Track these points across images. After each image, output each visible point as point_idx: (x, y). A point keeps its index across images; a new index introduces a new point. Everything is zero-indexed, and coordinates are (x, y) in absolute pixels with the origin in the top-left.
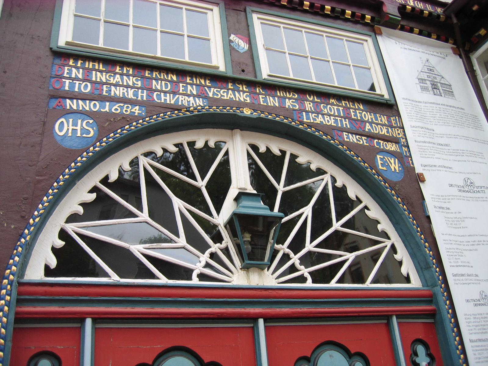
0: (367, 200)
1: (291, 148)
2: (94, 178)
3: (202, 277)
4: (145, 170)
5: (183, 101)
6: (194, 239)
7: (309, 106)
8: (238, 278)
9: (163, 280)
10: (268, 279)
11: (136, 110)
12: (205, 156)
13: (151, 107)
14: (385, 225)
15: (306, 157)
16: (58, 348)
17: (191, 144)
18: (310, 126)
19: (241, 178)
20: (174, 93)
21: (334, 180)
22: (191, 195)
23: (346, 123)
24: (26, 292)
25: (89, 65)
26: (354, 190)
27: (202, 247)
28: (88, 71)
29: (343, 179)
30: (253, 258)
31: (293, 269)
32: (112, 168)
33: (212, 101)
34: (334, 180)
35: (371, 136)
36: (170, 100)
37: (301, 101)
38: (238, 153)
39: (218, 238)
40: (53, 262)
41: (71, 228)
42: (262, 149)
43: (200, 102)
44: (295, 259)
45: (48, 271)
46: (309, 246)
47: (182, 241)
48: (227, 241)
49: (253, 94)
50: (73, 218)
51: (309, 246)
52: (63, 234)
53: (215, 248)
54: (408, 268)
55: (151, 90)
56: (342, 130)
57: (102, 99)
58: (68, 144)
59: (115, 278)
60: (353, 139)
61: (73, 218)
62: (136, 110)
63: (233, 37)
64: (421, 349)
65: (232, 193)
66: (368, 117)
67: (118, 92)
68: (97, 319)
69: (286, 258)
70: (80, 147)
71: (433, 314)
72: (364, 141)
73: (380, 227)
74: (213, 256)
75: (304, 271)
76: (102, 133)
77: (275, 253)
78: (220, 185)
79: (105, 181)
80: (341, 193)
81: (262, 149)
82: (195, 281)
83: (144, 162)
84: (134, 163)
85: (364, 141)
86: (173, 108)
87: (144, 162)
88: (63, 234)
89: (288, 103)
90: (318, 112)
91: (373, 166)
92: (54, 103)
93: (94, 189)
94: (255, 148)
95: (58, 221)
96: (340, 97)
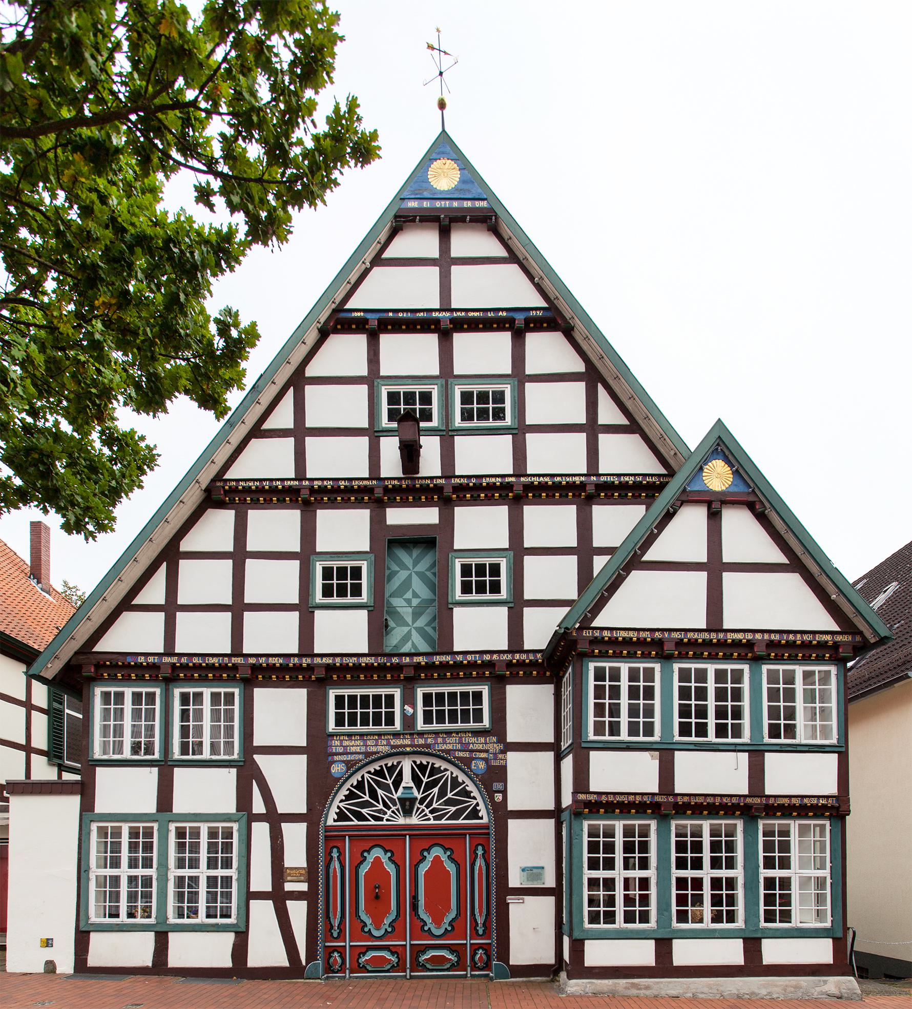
0: (468, 782)
1: (432, 760)
2: (348, 785)
3: (387, 820)
4: (368, 781)
5: (380, 748)
6: (385, 805)
7: (440, 740)
8: (401, 821)
9: (373, 822)
10: (414, 820)
11: (361, 757)
12: (391, 770)
13: (367, 754)
14: (475, 793)
15: (438, 763)
16: (339, 845)
17: (386, 765)
18: (439, 751)
19: (407, 780)
20: (376, 745)
21: (452, 773)
22: (386, 788)
23: (459, 747)
24: (328, 829)
25: (342, 738)
26: (461, 777)
27: (389, 808)
28: (341, 741)
29: (456, 772)
30: (408, 812)
31: (426, 815)
32: (354, 781)
33: (393, 747)
34: (452, 773)
35: (472, 751)
36: (374, 749)
37: (436, 739)
38: (407, 766)
39: (395, 805)
40: (336, 817)
41: (341, 805)
42: (418, 763)
43: (387, 748)
44: (427, 811)
45: (335, 821)
46: (435, 805)
47: (381, 807)
48: (398, 806)
49: (413, 739)
50: (341, 801)
51: (435, 805)
52: (338, 807)
53: (393, 808)
54: (483, 812)
55: (366, 746)
56: (455, 750)
57: (347, 754)
58: (336, 776)
59: (356, 822)
60: (461, 754)
61: (341, 801)
62: (361, 757)
63: (406, 707)
64: (480, 848)
65: (403, 784)
66: (473, 740)
67: (353, 749)
68: (350, 836)
69: (423, 810)
70: (339, 776)
71: (488, 834)
72: (467, 755)
73: (472, 795)
74: (393, 812)
75: (430, 816)
76: (348, 769)
77: (418, 809)
78: (397, 783)
79: (352, 786)
80: (455, 780)
81: (418, 763)
82: (385, 822)
83: (366, 776)
84: (363, 777)
85: (467, 755)
86: (375, 753)
87: (366, 776)
88: (338, 807)
89: (429, 741)
90: (444, 743)
91: (469, 767)
92: (330, 758)
93: (348, 789)
94: (415, 762)
95: (336, 802)
96: (457, 733)
